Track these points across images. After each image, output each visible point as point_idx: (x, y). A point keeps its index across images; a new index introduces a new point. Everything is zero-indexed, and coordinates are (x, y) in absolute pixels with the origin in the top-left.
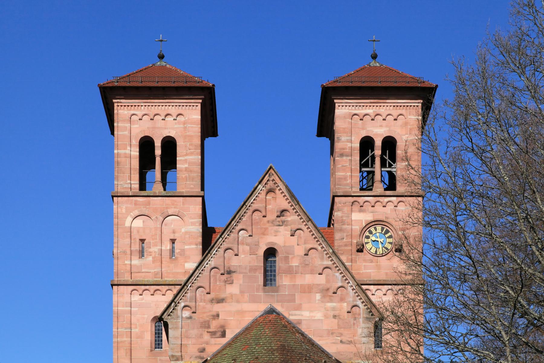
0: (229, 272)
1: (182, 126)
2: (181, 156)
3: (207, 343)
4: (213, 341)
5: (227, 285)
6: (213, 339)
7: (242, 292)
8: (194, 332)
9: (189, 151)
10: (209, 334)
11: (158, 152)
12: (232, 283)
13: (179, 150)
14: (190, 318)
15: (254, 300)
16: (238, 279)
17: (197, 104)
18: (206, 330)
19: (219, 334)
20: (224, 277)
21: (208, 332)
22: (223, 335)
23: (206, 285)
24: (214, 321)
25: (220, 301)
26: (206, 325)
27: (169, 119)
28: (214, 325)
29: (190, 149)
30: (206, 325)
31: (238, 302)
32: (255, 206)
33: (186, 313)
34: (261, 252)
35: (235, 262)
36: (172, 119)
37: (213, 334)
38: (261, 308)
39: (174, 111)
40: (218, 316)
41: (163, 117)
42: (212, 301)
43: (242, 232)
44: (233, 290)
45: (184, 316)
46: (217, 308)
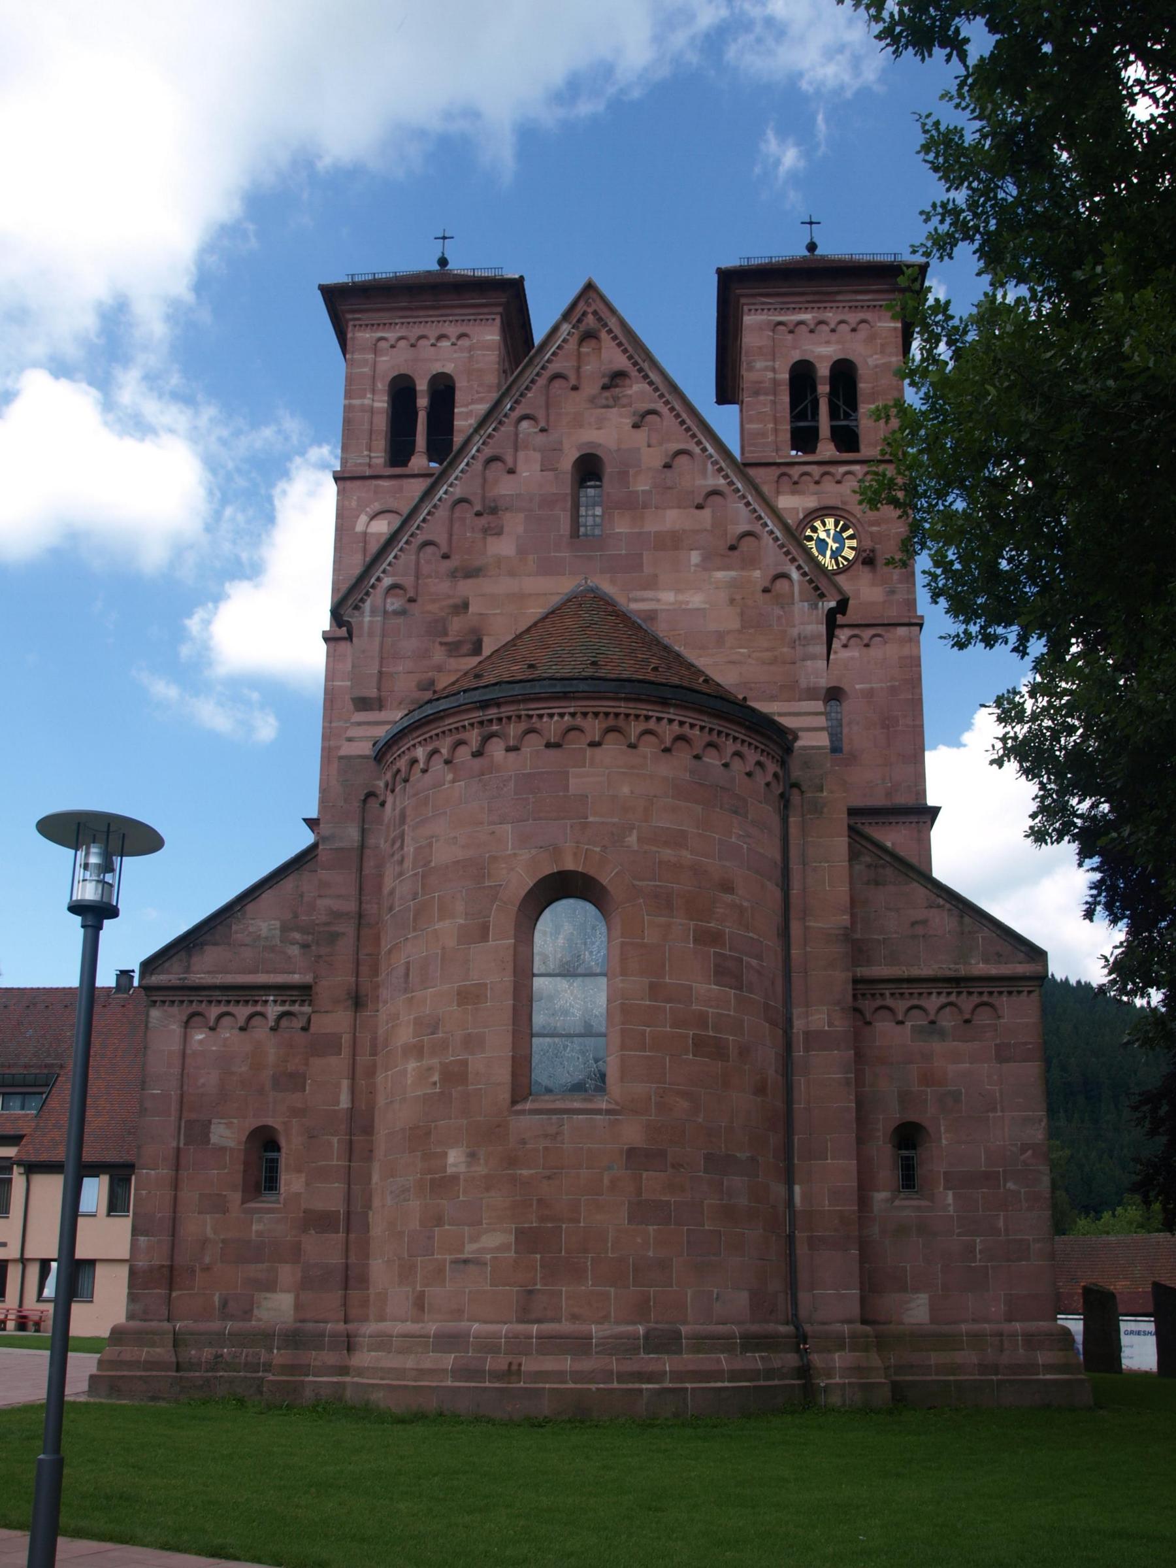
0: (494, 511)
1: (466, 355)
2: (461, 406)
3: (439, 669)
4: (453, 663)
5: (490, 539)
6: (452, 660)
7: (522, 552)
8: (409, 645)
9: (477, 396)
10: (443, 648)
11: (423, 402)
12: (499, 533)
13: (459, 396)
14: (402, 613)
15: (548, 568)
16: (515, 524)
17: (493, 317)
18: (439, 640)
19: (467, 648)
20: (483, 521)
21: (441, 644)
22: (477, 649)
23: (441, 539)
24: (455, 619)
25: (472, 573)
26: (437, 628)
27: (445, 344)
28: (456, 626)
29: (478, 392)
30: (437, 628)
31: (512, 574)
32: (554, 367)
33: (393, 604)
34: (567, 462)
35: (505, 487)
36: (449, 344)
37: (453, 649)
38: (564, 586)
39: (452, 330)
40: (465, 606)
41: (433, 341)
42: (453, 575)
43: (525, 424)
44: (503, 547)
45: (390, 608)
46: (465, 588)
